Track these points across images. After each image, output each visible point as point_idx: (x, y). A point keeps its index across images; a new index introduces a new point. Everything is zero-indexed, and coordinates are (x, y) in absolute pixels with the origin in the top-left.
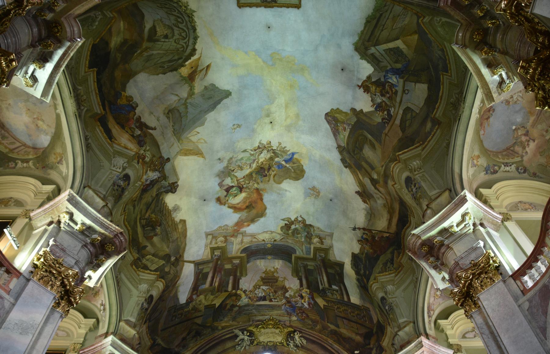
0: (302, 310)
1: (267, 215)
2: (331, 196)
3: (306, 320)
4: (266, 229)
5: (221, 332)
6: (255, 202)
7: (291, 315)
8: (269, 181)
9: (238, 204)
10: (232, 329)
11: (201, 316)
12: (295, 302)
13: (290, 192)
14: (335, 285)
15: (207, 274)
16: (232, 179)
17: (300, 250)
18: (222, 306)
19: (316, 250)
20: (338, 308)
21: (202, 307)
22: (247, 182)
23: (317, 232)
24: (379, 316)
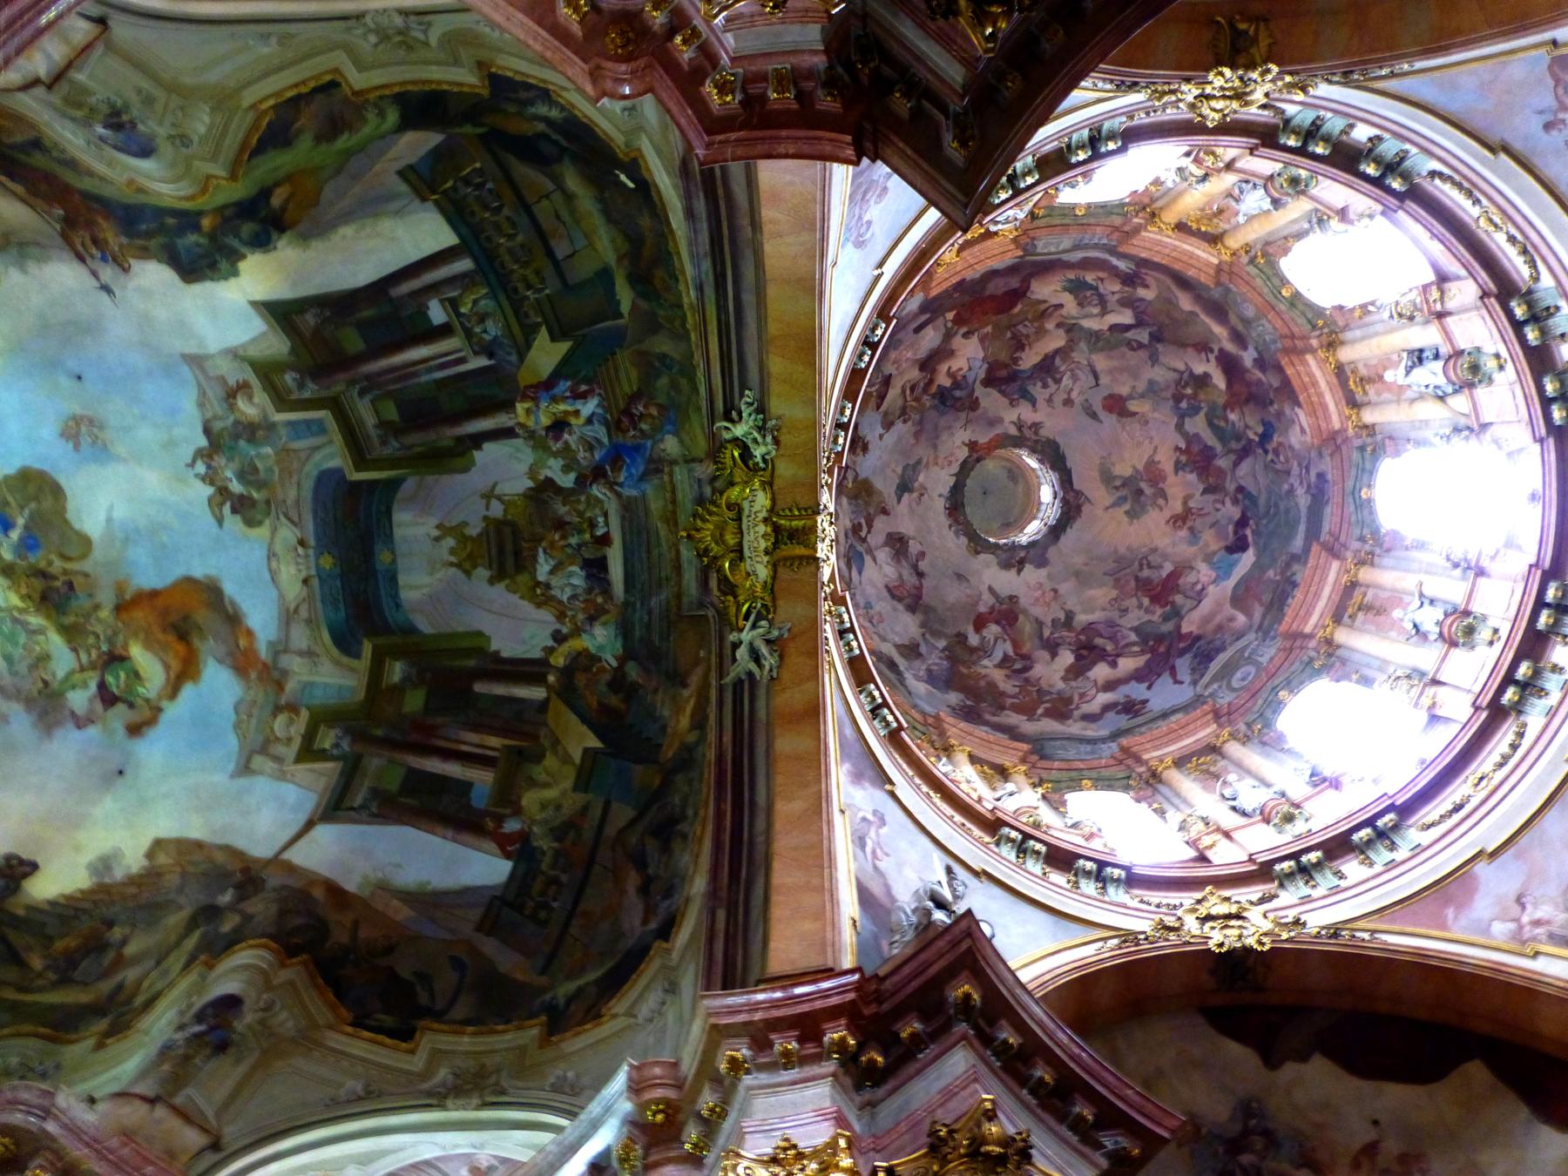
0: (620, 418)
1: (213, 572)
2: (65, 382)
3: (661, 400)
4: (262, 576)
5: (712, 736)
6: (164, 613)
7: (660, 460)
8: (86, 575)
9: (167, 667)
10: (721, 689)
11: (607, 804)
12: (591, 448)
13: (111, 508)
14: (423, 313)
15: (414, 776)
16: (73, 687)
17: (317, 457)
18: (603, 722)
19: (282, 400)
20: (529, 287)
21: (580, 799)
22: (91, 640)
23: (217, 408)
24: (367, 130)
